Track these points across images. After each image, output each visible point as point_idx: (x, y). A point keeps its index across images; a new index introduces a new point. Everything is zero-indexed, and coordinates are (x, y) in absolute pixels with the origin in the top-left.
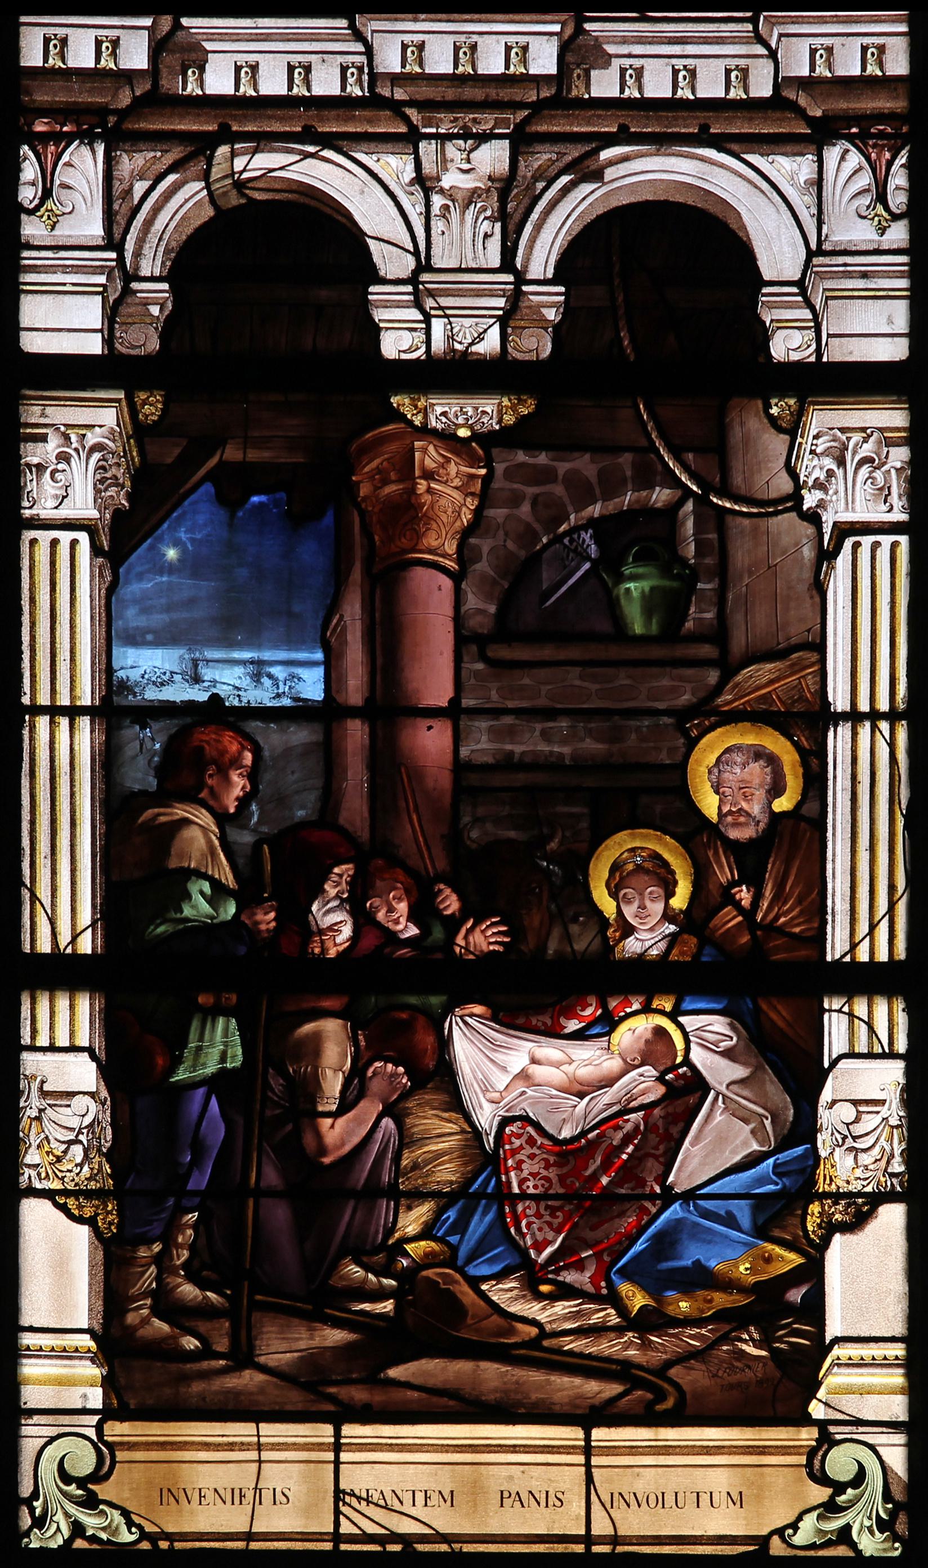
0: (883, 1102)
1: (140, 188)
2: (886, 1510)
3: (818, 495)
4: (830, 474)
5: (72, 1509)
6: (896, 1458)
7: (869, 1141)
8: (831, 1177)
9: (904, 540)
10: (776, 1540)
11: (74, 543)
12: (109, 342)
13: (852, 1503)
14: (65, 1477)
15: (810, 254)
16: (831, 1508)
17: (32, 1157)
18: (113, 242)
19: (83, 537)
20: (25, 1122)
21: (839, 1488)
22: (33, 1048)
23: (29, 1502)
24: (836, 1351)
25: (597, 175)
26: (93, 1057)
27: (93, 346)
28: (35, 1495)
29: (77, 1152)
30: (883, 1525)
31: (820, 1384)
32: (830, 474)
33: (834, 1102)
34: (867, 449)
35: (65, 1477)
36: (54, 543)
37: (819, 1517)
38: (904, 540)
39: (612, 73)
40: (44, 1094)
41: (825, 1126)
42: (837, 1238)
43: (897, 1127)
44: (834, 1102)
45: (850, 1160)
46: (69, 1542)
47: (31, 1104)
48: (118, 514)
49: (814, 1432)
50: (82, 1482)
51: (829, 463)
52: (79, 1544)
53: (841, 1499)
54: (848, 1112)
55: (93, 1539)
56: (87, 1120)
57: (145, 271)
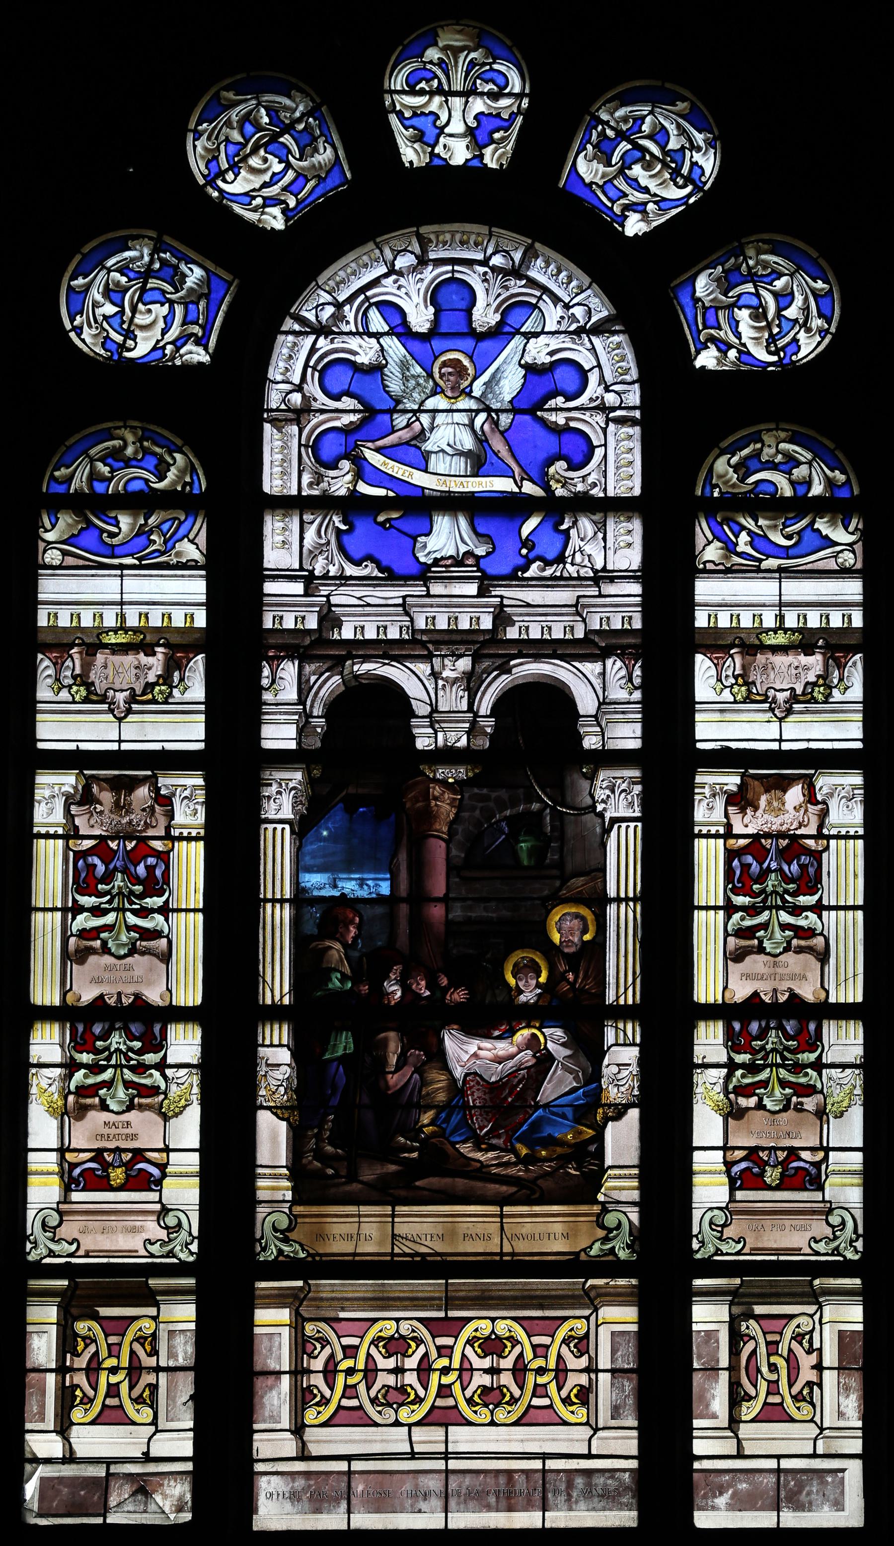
0: (629, 1065)
3: (603, 805)
4: (608, 796)
5: (278, 1243)
6: (635, 1217)
7: (624, 1081)
9: (639, 824)
10: (583, 1253)
11: (283, 829)
12: (299, 744)
13: (615, 1237)
14: (275, 1230)
15: (600, 704)
17: (262, 1092)
18: (301, 701)
19: (287, 827)
20: (259, 1077)
21: (610, 1230)
22: (263, 1045)
23: (259, 1241)
24: (609, 1172)
25: (509, 671)
27: (293, 745)
28: (262, 1238)
29: (282, 1090)
30: (628, 1246)
32: (608, 796)
34: (624, 786)
35: (275, 1230)
36: (275, 829)
38: (639, 824)
40: (268, 1065)
45: (616, 1090)
46: (276, 1258)
47: (262, 1070)
48: (302, 817)
49: (600, 1207)
50: (282, 1232)
51: (608, 792)
52: (281, 1258)
54: (615, 1069)
55: (288, 1256)
57: (315, 713)
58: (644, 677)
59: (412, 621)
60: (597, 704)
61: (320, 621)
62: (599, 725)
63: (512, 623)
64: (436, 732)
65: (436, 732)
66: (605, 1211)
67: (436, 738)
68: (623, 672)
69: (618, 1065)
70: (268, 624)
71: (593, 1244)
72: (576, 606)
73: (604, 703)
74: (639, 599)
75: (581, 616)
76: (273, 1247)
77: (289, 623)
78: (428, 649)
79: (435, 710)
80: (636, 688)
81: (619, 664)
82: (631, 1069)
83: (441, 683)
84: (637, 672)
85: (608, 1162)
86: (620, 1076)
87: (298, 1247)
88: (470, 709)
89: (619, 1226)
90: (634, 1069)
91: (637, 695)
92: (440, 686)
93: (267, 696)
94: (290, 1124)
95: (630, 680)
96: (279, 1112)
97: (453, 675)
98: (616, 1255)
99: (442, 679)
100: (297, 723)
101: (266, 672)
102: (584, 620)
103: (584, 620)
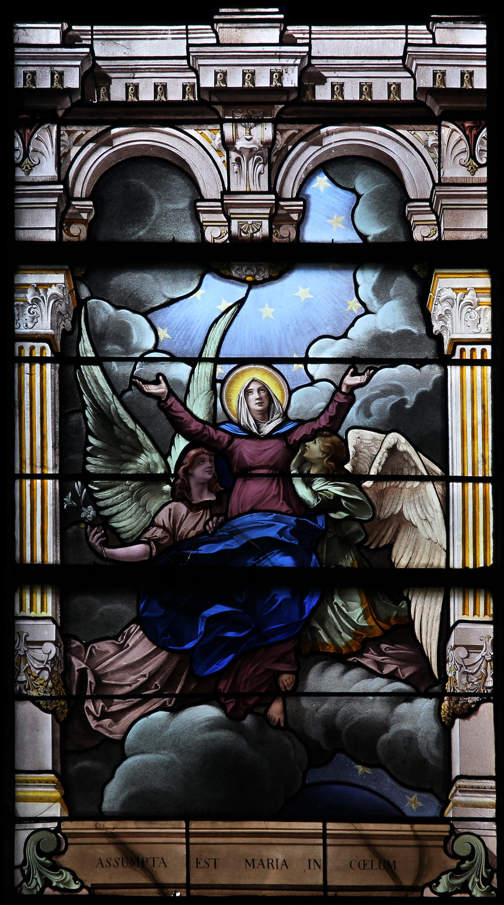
0: (481, 648)
1: (75, 150)
2: (487, 873)
8: (454, 688)
12: (59, 236)
16: (457, 872)
26: (54, 622)
31: (450, 801)
33: (456, 646)
37: (451, 877)
39: (328, 85)
40: (28, 643)
41: (450, 660)
42: (457, 721)
43: (490, 661)
44: (456, 646)
53: (464, 866)
54: (463, 653)
56: (52, 656)
58: (490, 151)
59: (198, 77)
60: (431, 185)
61: (83, 79)
62: (434, 212)
63: (323, 80)
64: (229, 220)
65: (229, 220)
66: (454, 834)
67: (229, 226)
68: (464, 145)
69: (467, 647)
70: (20, 84)
71: (440, 878)
72: (403, 58)
73: (440, 184)
74: (484, 50)
75: (410, 71)
76: (37, 876)
77: (44, 83)
78: (217, 113)
79: (226, 192)
80: (481, 166)
81: (458, 135)
82: (483, 653)
83: (234, 155)
84: (481, 144)
85: (456, 771)
86: (468, 662)
87: (69, 877)
88: (271, 191)
89: (472, 856)
90: (488, 652)
91: (483, 174)
92: (233, 160)
93: (20, 174)
94: (55, 719)
95: (472, 156)
96: (42, 702)
97: (249, 145)
98: (470, 892)
99: (236, 151)
100: (57, 209)
101: (18, 144)
102: (413, 76)
103: (413, 76)
